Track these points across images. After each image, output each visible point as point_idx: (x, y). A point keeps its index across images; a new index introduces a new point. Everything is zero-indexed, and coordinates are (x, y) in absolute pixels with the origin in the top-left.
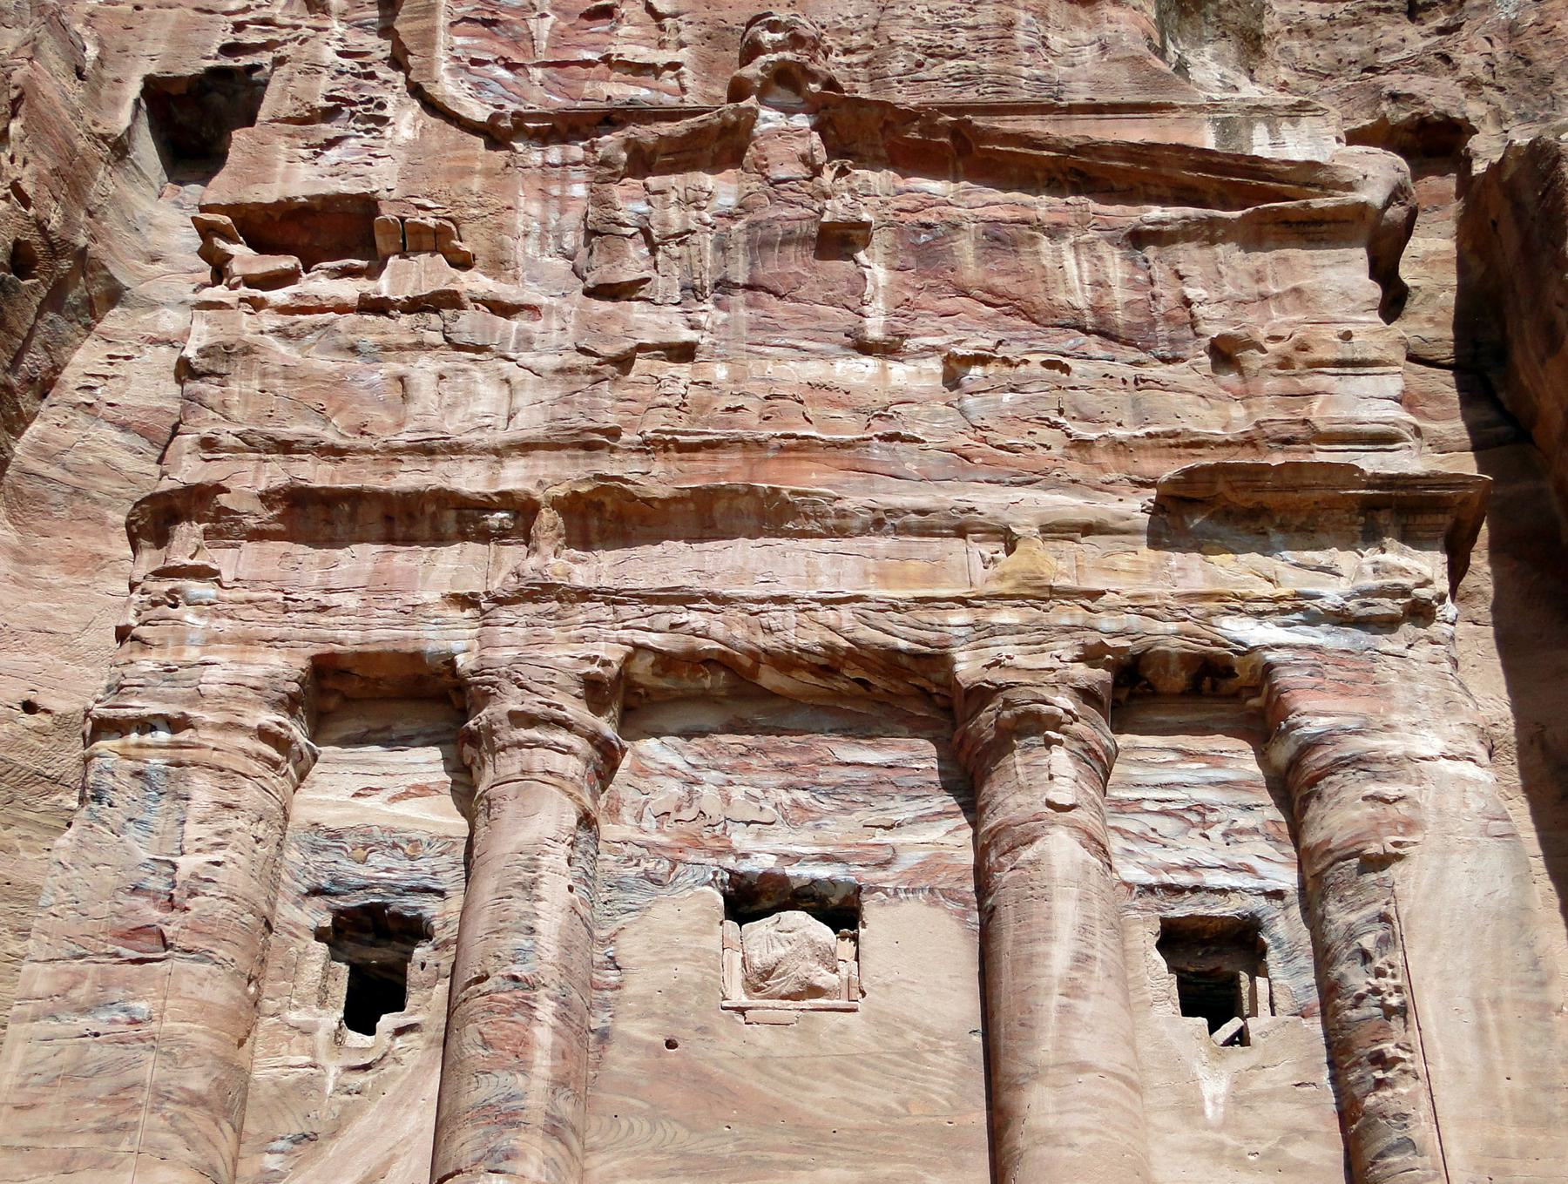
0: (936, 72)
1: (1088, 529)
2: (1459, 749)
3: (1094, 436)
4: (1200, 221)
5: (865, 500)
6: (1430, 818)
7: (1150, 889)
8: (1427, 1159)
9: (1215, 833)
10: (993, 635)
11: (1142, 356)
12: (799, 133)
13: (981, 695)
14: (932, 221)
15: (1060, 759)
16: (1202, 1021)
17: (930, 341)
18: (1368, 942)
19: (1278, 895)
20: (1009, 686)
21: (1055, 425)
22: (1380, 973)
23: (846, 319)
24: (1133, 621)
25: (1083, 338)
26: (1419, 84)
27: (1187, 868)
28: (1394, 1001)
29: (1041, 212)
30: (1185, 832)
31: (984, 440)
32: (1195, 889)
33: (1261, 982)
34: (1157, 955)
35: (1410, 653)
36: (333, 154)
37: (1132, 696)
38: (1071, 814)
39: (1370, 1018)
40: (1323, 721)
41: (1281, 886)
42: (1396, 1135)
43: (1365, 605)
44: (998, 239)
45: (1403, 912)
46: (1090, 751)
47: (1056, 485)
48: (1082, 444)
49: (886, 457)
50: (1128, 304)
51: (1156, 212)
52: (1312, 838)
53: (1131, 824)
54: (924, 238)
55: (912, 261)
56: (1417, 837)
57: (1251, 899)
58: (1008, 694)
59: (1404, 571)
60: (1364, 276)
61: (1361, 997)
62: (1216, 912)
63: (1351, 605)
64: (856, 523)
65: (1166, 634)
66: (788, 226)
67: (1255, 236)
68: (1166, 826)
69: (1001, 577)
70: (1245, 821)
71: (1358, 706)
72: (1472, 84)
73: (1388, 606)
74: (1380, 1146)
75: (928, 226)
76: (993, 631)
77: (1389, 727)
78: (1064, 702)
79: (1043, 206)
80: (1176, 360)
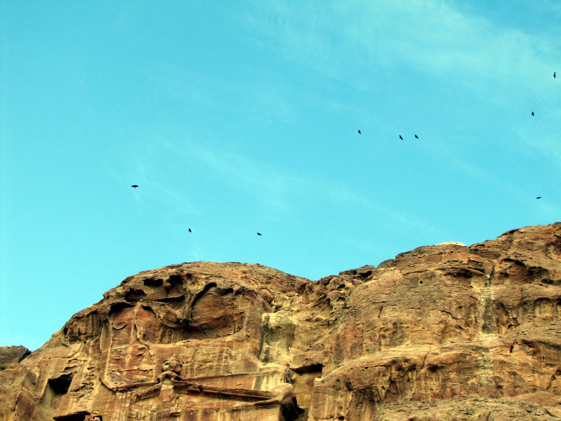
0: (204, 367)
12: (170, 390)
14: (193, 409)
36: (82, 399)
54: (191, 414)
66: (165, 413)
67: (258, 406)
75: (192, 411)
79: (215, 402)
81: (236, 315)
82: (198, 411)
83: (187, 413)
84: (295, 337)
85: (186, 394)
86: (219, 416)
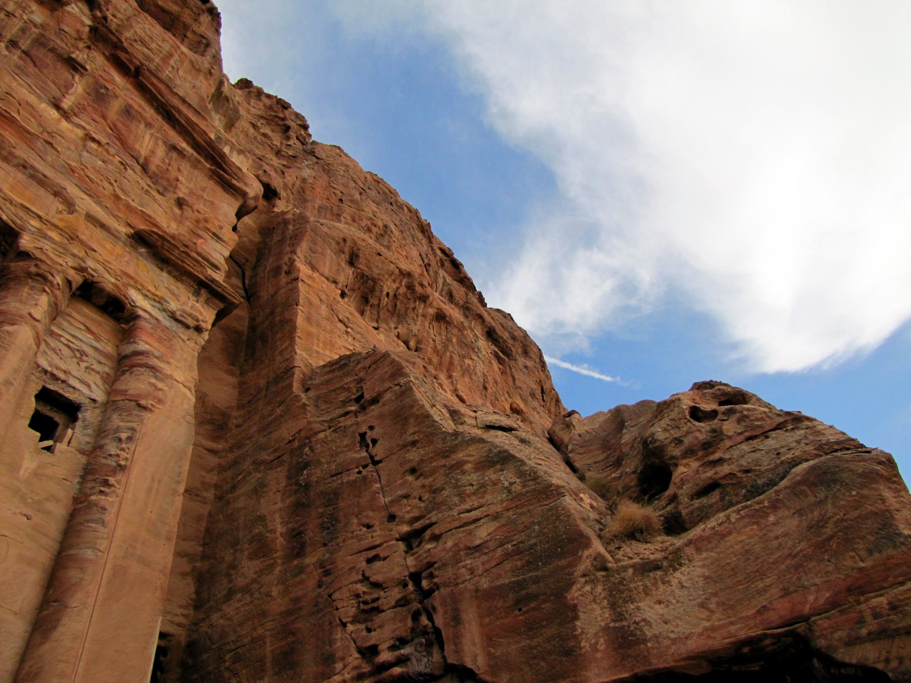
0: (139, 48)
1: (103, 226)
2: (188, 384)
3: (123, 197)
4: (196, 159)
5: (24, 156)
6: (168, 402)
7: (46, 372)
8: (107, 530)
9: (83, 365)
10: (45, 238)
11: (152, 185)
13: (25, 255)
15: (44, 300)
16: (39, 434)
17: (83, 124)
18: (124, 436)
19: (94, 401)
20: (41, 260)
21: (111, 184)
22: (123, 450)
23: (58, 94)
24: (100, 268)
25: (136, 164)
26: (273, 174)
27: (65, 372)
28: (123, 463)
29: (148, 115)
30: (72, 358)
31: (83, 170)
32: (64, 382)
33: (70, 431)
34: (33, 399)
35: (188, 342)
37: (80, 296)
38: (36, 323)
39: (109, 466)
40: (147, 346)
41: (97, 399)
42: (98, 516)
43: (182, 316)
44: (128, 112)
45: (143, 431)
46: (56, 304)
47: (99, 203)
48: (117, 197)
49: (42, 148)
50: (158, 166)
51: (184, 145)
52: (120, 386)
53: (53, 343)
54: (102, 91)
55: (93, 94)
56: (160, 407)
57: (82, 398)
58: (39, 263)
59: (201, 314)
60: (234, 214)
61: (110, 455)
62: (67, 395)
63: (178, 313)
64: (16, 161)
65: (108, 282)
68: (66, 352)
69: (61, 220)
70: (96, 366)
71: (162, 350)
72: (285, 185)
73: (191, 322)
74: (88, 517)
76: (45, 237)
77: (168, 363)
78: (59, 279)
79: (150, 113)
80: (162, 194)
81: (194, 32)
82: (116, 97)
83: (96, 83)
84: (233, 129)
85: (104, 54)
86: (147, 137)
